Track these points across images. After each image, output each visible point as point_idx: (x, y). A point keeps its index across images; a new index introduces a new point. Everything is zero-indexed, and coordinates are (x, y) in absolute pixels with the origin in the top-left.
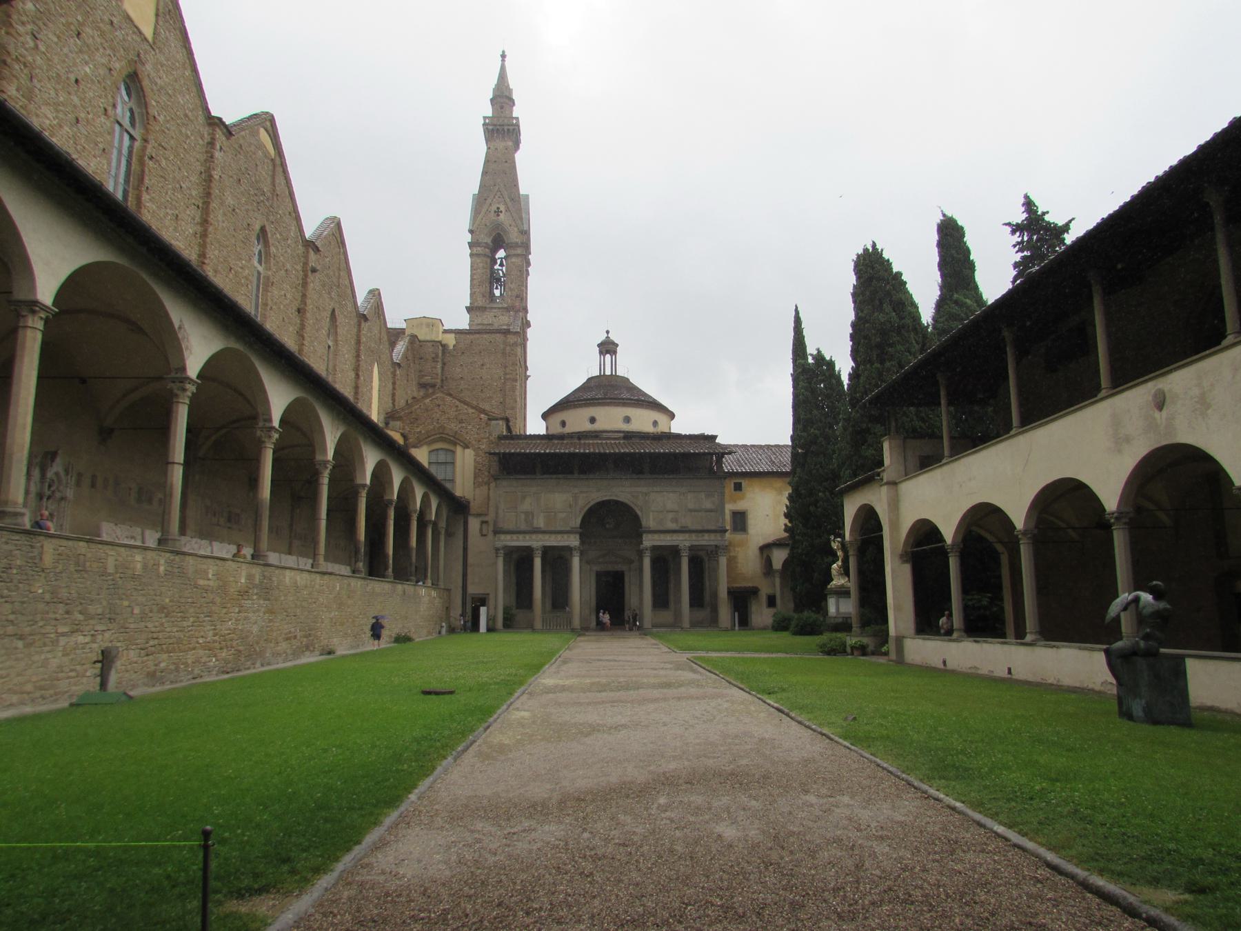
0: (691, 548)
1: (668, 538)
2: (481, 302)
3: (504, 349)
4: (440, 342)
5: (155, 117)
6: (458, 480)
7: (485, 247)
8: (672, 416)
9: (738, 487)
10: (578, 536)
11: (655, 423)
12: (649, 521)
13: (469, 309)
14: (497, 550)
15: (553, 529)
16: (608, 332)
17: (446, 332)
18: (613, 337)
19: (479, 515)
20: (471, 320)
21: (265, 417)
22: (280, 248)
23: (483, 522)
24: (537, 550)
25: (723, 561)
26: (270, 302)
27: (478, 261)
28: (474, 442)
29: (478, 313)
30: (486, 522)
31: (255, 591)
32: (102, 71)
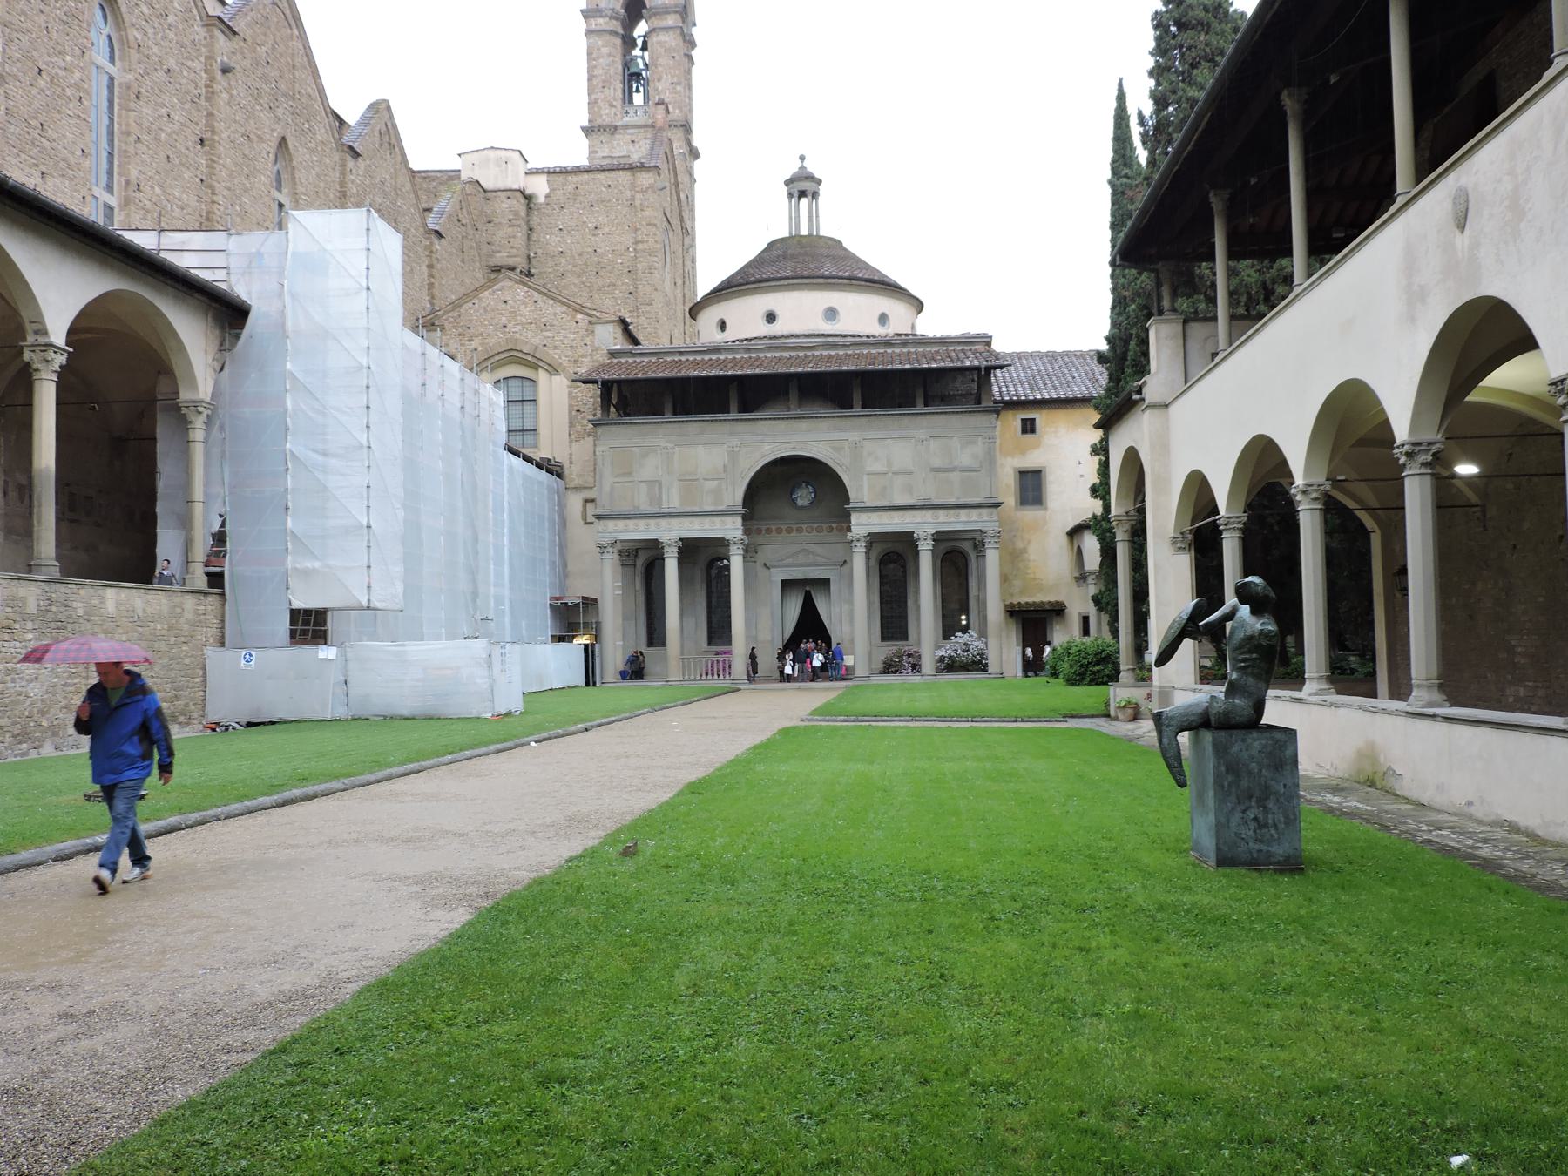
0: (940, 537)
1: (896, 520)
2: (607, 116)
3: (633, 198)
4: (522, 192)
6: (544, 431)
7: (611, 17)
8: (919, 306)
9: (1029, 427)
10: (739, 520)
11: (883, 318)
12: (860, 490)
13: (588, 131)
14: (601, 546)
15: (696, 509)
16: (802, 158)
17: (530, 173)
18: (812, 167)
19: (578, 489)
20: (592, 152)
21: (35, 327)
22: (150, 31)
23: (586, 501)
24: (669, 545)
25: (992, 557)
26: (134, 129)
27: (600, 43)
29: (602, 138)
30: (593, 501)
31: (30, 625)
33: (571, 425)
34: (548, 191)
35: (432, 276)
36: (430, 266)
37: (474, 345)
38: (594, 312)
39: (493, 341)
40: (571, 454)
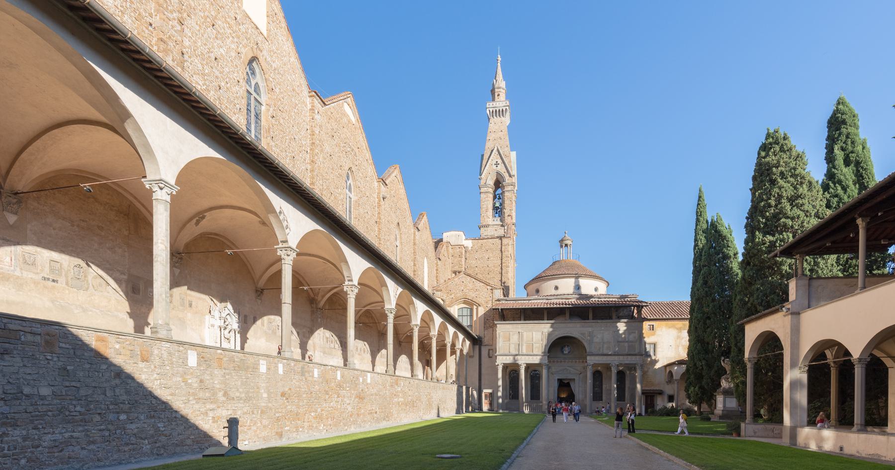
5: (273, 89)
23: (489, 350)
28: (483, 303)
32: (233, 54)
33: (485, 324)
34: (472, 246)
35: (437, 273)
36: (437, 270)
37: (452, 296)
38: (493, 286)
39: (459, 295)
40: (484, 334)
